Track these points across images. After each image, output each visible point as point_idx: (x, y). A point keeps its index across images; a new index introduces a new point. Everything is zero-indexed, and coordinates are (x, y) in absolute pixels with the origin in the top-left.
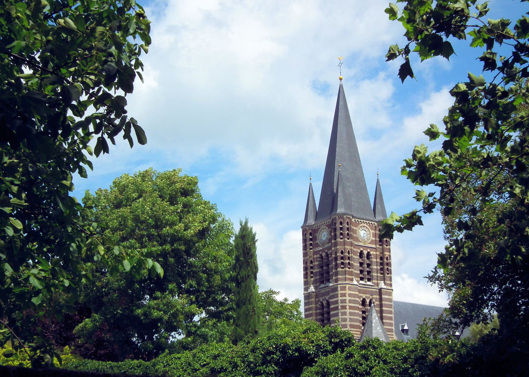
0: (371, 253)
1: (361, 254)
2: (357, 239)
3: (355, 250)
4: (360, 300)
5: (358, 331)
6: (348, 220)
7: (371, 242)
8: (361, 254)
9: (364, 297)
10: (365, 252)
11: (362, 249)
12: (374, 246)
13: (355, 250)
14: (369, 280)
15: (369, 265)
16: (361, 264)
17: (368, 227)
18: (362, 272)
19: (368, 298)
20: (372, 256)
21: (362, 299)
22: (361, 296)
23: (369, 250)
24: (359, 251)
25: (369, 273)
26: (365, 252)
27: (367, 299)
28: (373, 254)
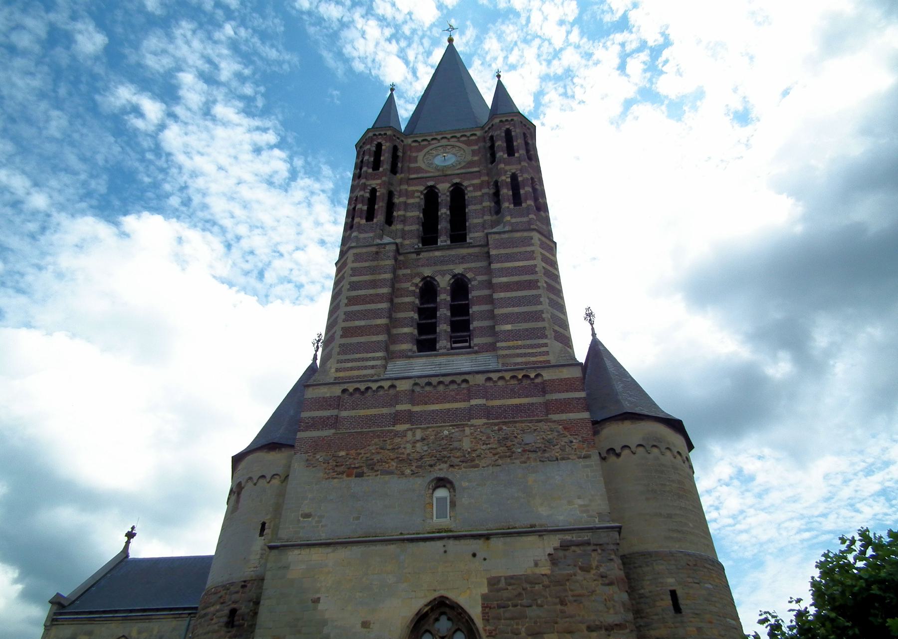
0: (465, 183)
1: (431, 195)
2: (419, 170)
4: (412, 285)
5: (374, 359)
9: (427, 272)
10: (444, 188)
11: (430, 183)
21: (417, 280)
22: (418, 274)
24: (422, 188)
26: (444, 188)
27: (438, 278)
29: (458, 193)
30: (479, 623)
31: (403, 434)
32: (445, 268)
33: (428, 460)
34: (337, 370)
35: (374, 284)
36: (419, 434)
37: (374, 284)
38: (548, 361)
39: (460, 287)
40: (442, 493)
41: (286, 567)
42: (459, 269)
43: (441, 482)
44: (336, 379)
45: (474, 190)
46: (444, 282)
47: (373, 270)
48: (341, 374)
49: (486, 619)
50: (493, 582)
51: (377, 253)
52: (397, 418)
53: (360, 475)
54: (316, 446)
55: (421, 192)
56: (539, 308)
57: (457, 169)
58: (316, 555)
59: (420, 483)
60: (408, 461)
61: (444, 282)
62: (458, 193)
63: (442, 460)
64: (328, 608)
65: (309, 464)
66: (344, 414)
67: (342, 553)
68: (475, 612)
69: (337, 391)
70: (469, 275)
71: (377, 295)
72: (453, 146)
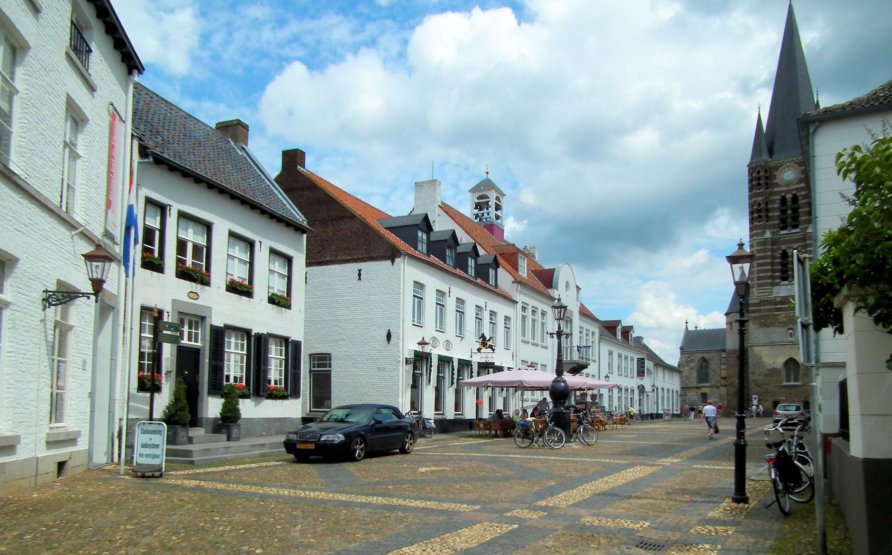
0: (798, 194)
1: (783, 200)
2: (777, 185)
3: (776, 197)
4: (778, 254)
6: (758, 169)
7: (800, 181)
9: (784, 247)
10: (789, 196)
13: (776, 197)
14: (795, 227)
15: (795, 210)
16: (783, 212)
17: (796, 165)
18: (783, 220)
20: (800, 198)
21: (780, 252)
23: (794, 192)
25: (795, 218)
26: (789, 196)
28: (800, 196)
29: (795, 199)
31: (779, 315)
33: (787, 323)
34: (758, 293)
35: (765, 257)
36: (784, 315)
37: (765, 257)
40: (791, 331)
41: (753, 351)
43: (791, 329)
45: (802, 200)
47: (764, 251)
48: (759, 295)
51: (765, 242)
52: (778, 310)
53: (768, 327)
54: (755, 318)
57: (796, 184)
58: (760, 348)
59: (785, 329)
60: (781, 323)
62: (795, 199)
63: (791, 323)
64: (765, 359)
65: (754, 324)
66: (762, 308)
67: (767, 347)
69: (758, 301)
71: (766, 263)
72: (793, 167)
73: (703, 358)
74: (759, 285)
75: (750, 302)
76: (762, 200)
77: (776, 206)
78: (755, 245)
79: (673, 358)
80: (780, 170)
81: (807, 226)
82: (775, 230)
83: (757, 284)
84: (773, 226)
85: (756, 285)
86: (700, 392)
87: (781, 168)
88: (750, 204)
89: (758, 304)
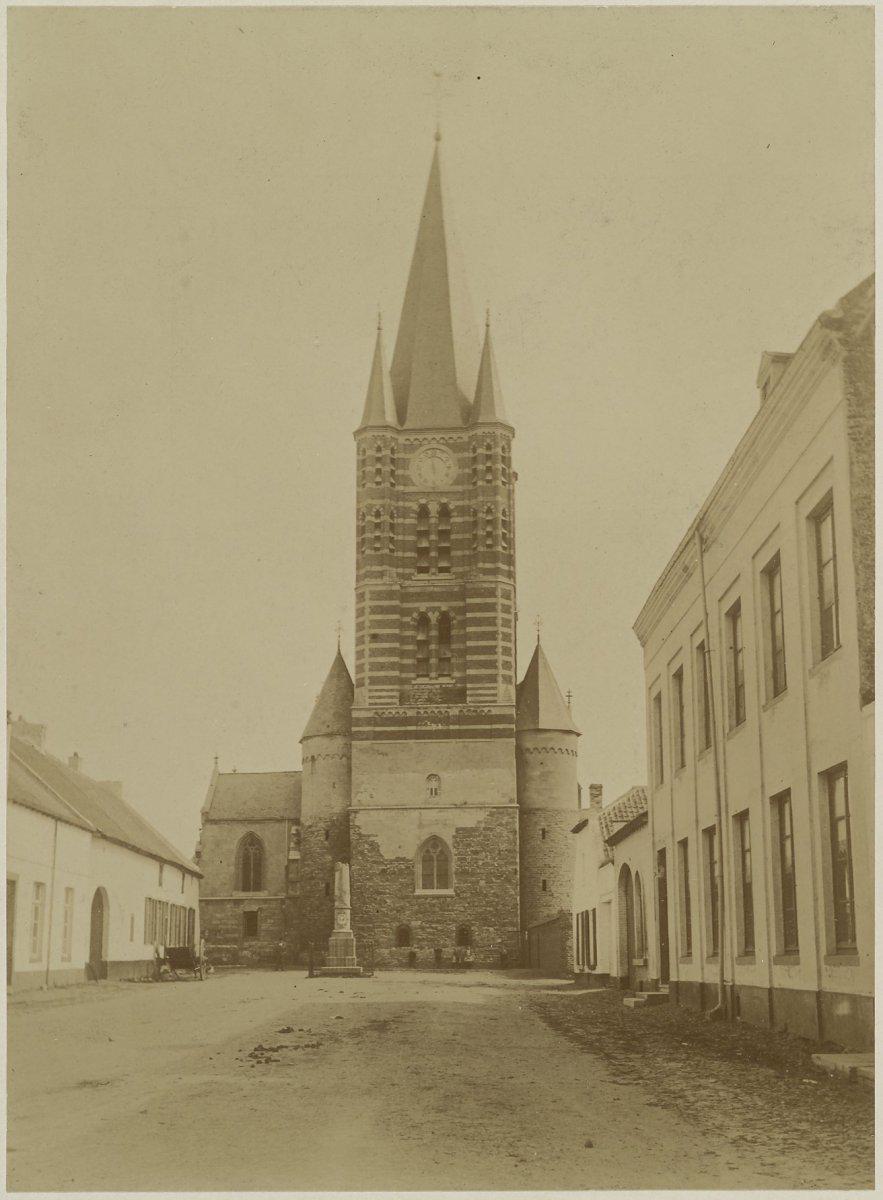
0: (451, 507)
8: (423, 512)
9: (423, 609)
10: (434, 508)
11: (423, 501)
12: (460, 488)
17: (443, 447)
19: (433, 609)
21: (415, 615)
22: (416, 609)
24: (415, 507)
26: (434, 508)
27: (430, 614)
30: (451, 847)
32: (436, 604)
38: (495, 701)
39: (445, 618)
42: (444, 607)
44: (370, 704)
46: (434, 617)
49: (457, 844)
50: (457, 830)
55: (414, 512)
56: (496, 657)
61: (434, 617)
62: (445, 512)
68: (449, 842)
69: (370, 714)
70: (452, 614)
73: (251, 835)
74: (374, 681)
75: (355, 714)
76: (383, 506)
77: (408, 521)
78: (367, 596)
79: (184, 837)
80: (417, 453)
81: (467, 568)
82: (407, 571)
83: (370, 678)
84: (403, 563)
85: (367, 681)
86: (240, 910)
87: (423, 448)
88: (358, 510)
89: (369, 721)
